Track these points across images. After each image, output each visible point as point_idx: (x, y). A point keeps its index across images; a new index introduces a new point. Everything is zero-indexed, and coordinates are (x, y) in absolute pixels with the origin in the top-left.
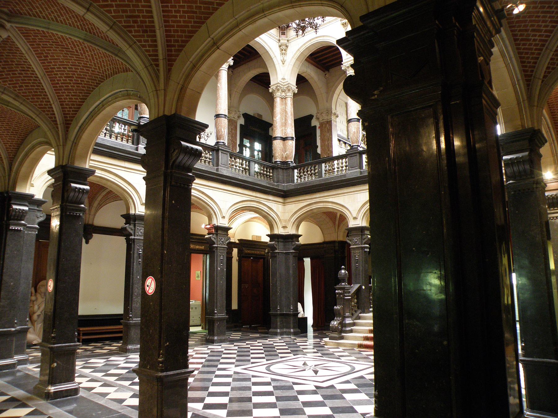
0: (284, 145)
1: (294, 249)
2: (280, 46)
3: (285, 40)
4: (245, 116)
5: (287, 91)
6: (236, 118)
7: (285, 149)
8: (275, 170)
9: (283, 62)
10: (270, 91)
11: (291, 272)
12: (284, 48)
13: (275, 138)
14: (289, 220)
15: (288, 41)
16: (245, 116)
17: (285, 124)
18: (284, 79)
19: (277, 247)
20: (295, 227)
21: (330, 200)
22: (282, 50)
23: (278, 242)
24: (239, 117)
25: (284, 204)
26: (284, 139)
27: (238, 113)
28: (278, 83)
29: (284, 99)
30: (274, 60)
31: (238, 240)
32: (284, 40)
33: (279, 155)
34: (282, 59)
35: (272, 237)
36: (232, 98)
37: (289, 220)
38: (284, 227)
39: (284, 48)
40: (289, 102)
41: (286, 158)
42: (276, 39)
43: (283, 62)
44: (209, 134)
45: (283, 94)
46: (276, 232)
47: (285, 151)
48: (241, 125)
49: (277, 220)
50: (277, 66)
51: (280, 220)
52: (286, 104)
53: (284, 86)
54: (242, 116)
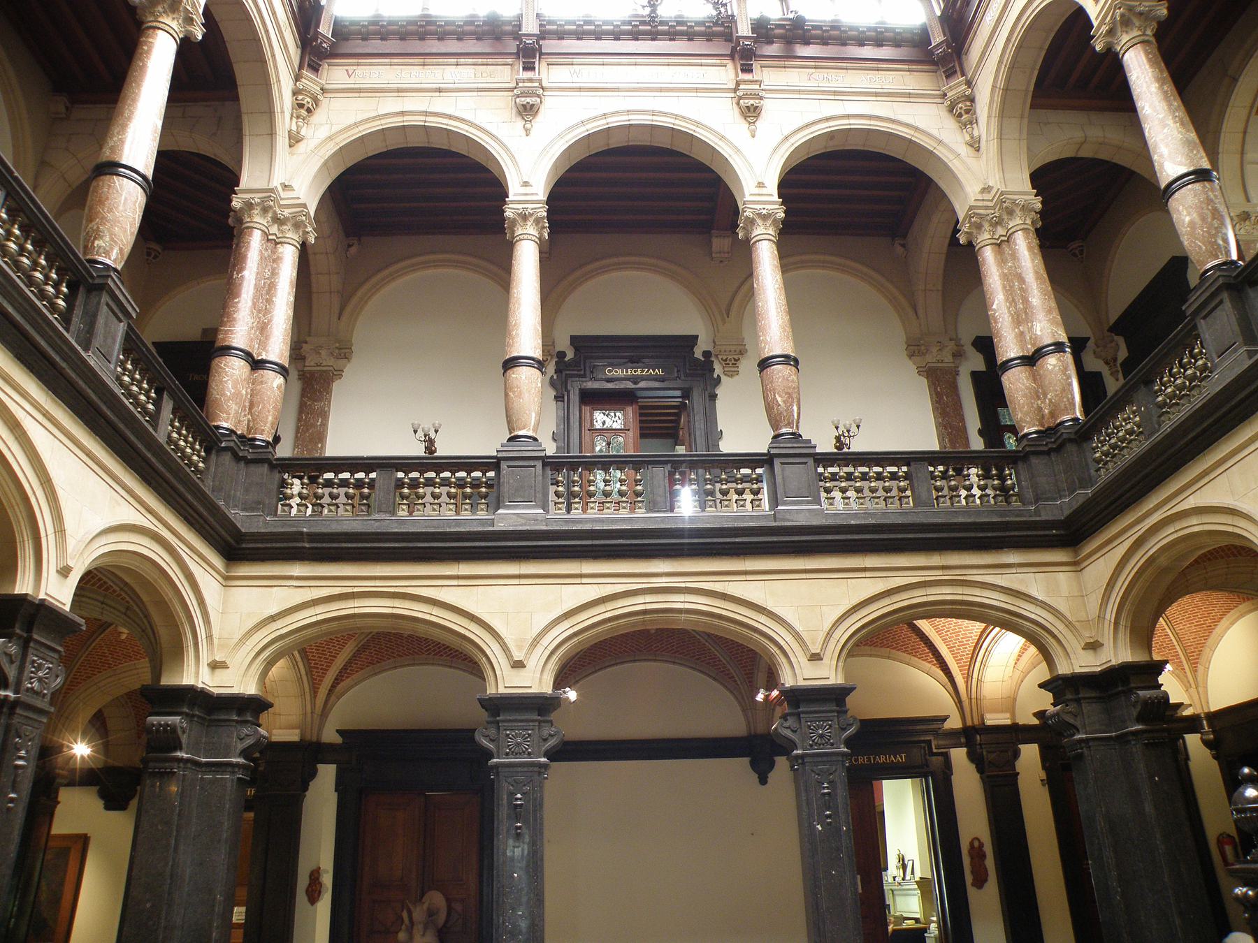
0: (1035, 378)
1: (1139, 719)
2: (951, 109)
3: (959, 85)
5: (1005, 217)
6: (948, 358)
7: (1039, 392)
8: (1020, 465)
11: (1148, 808)
14: (1101, 618)
17: (1022, 318)
18: (986, 189)
19: (1078, 723)
20: (1124, 637)
21: (1192, 502)
22: (960, 115)
23: (1078, 701)
24: (958, 354)
25: (1076, 565)
28: (971, 208)
31: (1036, 715)
33: (1027, 414)
34: (968, 138)
35: (1059, 686)
36: (921, 312)
37: (1101, 618)
38: (1093, 646)
39: (962, 110)
41: (1053, 415)
42: (934, 96)
43: (975, 145)
44: (854, 429)
45: (1000, 231)
46: (1063, 669)
47: (1045, 395)
49: (1058, 627)
51: (1069, 624)
52: (1014, 256)
53: (993, 208)
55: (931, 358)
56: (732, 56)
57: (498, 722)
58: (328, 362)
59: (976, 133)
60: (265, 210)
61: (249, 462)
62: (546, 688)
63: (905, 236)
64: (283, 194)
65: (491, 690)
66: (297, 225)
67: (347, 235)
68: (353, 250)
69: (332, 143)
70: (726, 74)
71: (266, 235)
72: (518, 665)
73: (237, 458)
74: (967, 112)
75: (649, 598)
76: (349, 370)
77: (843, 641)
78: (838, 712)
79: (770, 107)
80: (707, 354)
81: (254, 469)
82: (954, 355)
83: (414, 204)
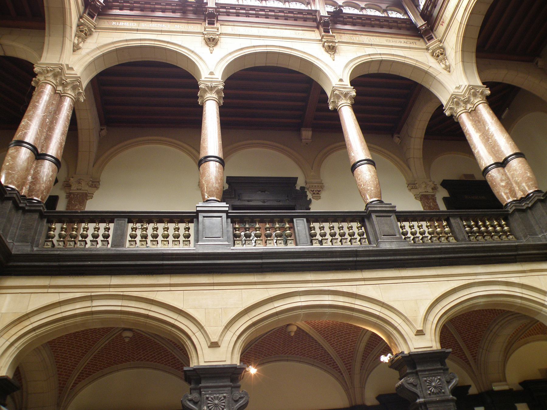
3: (435, 42)
4: (445, 184)
6: (430, 190)
9: (448, 69)
10: (447, 113)
12: (440, 54)
13: (486, 170)
15: (441, 41)
16: (445, 184)
22: (438, 56)
24: (434, 189)
26: (503, 164)
27: (431, 183)
28: (452, 95)
29: (473, 113)
30: (431, 71)
32: (433, 44)
34: (443, 66)
40: (486, 113)
42: (423, 49)
43: (448, 69)
45: (469, 106)
48: (445, 199)
50: (440, 77)
54: (440, 188)
55: (421, 190)
56: (318, 28)
57: (200, 388)
58: (85, 188)
59: (447, 64)
60: (55, 76)
61: (25, 211)
62: (236, 361)
63: (399, 133)
64: (68, 72)
65: (194, 364)
66: (74, 88)
67: (101, 124)
68: (104, 132)
69: (99, 51)
70: (316, 35)
71: (55, 90)
72: (214, 345)
73: (17, 207)
74: (442, 54)
75: (303, 298)
76: (96, 194)
77: (435, 322)
78: (444, 370)
79: (342, 48)
80: (302, 188)
81: (28, 216)
82: (433, 189)
83: (142, 101)
